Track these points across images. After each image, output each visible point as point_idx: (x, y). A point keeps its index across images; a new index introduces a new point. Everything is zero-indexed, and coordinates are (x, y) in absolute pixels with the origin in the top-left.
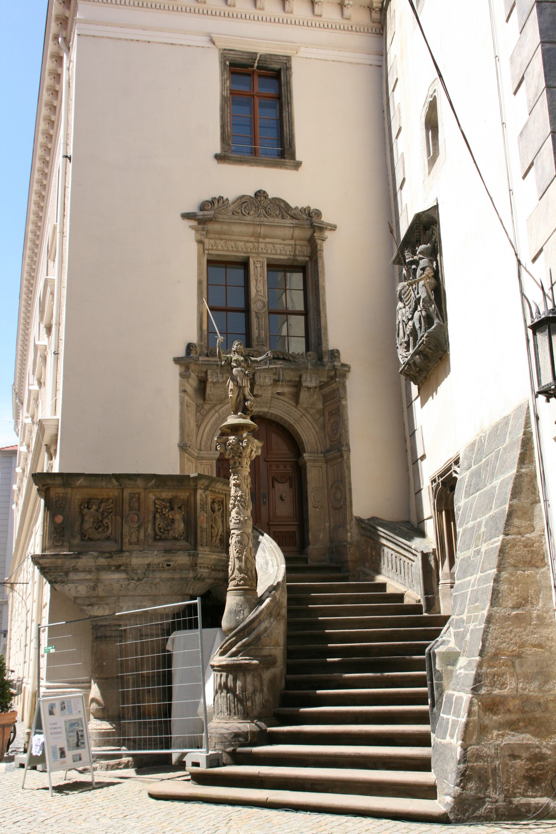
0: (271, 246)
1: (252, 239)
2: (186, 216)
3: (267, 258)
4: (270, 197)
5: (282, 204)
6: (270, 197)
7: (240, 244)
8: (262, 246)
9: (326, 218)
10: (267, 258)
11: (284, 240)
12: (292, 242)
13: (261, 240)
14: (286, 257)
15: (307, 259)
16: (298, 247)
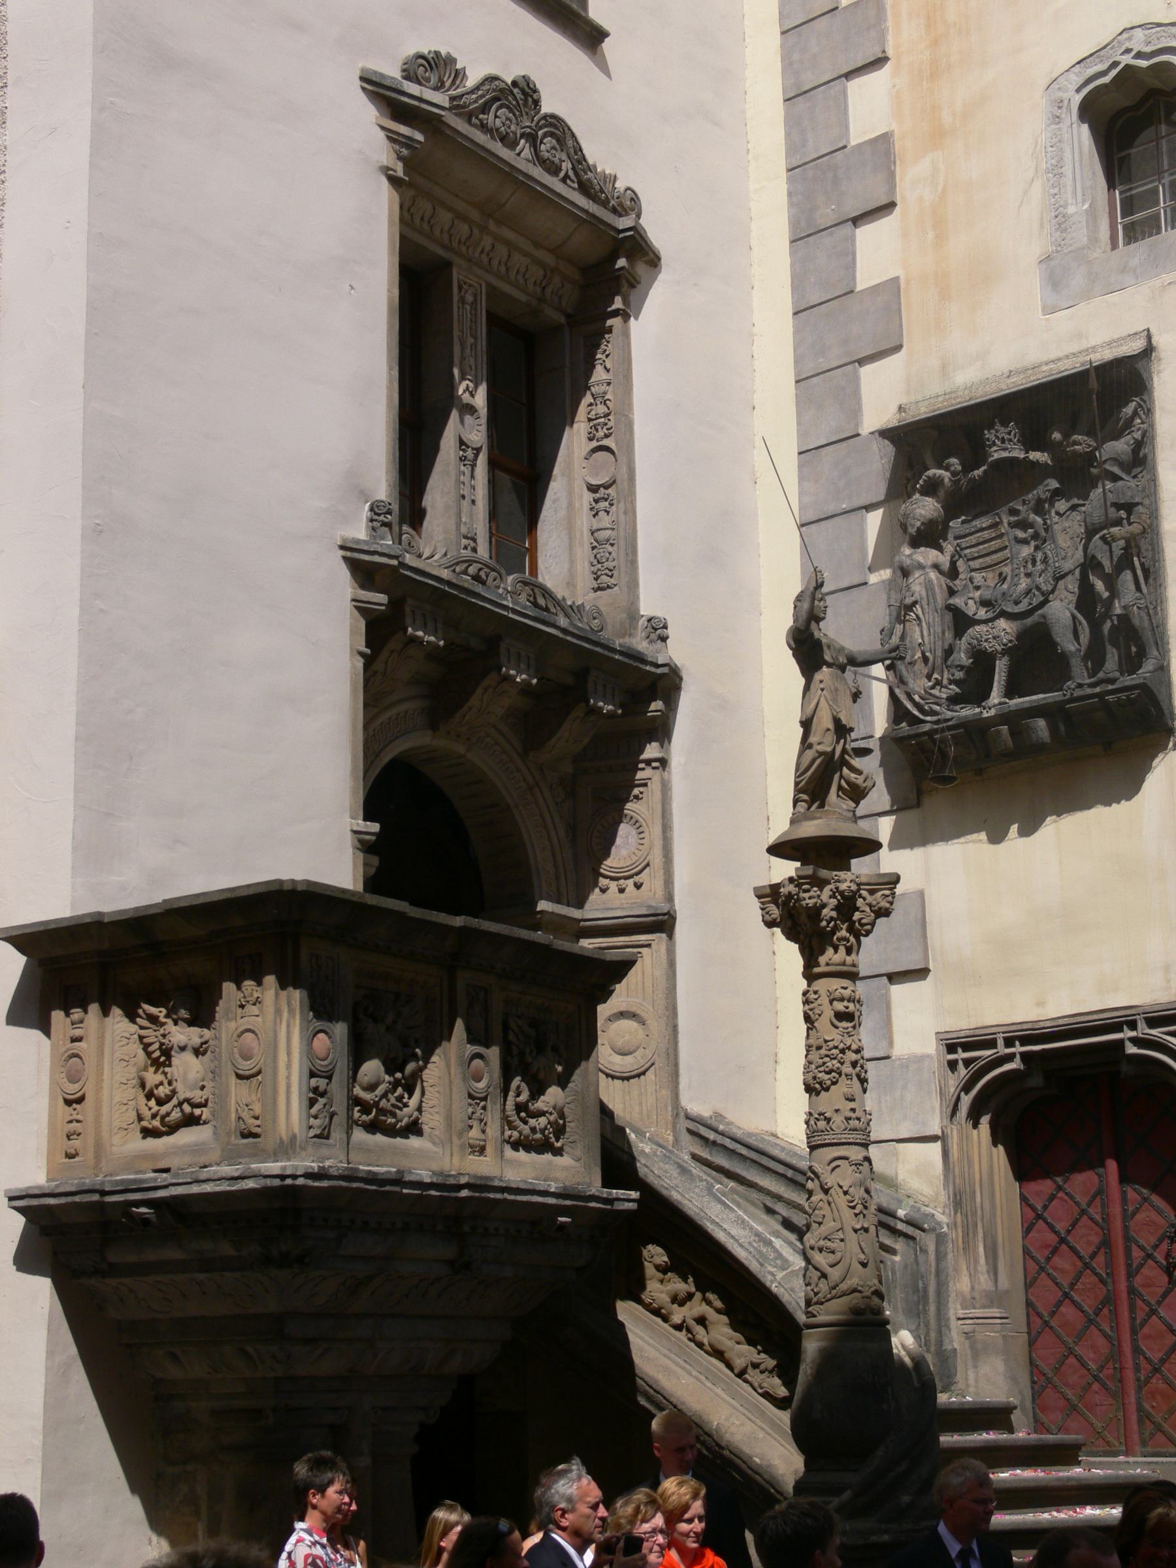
0: (503, 251)
1: (474, 214)
2: (377, 89)
3: (488, 284)
4: (546, 108)
5: (570, 143)
6: (546, 108)
7: (445, 217)
8: (487, 242)
9: (657, 226)
10: (488, 284)
11: (536, 245)
12: (550, 259)
13: (492, 226)
14: (523, 298)
15: (563, 320)
16: (557, 280)
